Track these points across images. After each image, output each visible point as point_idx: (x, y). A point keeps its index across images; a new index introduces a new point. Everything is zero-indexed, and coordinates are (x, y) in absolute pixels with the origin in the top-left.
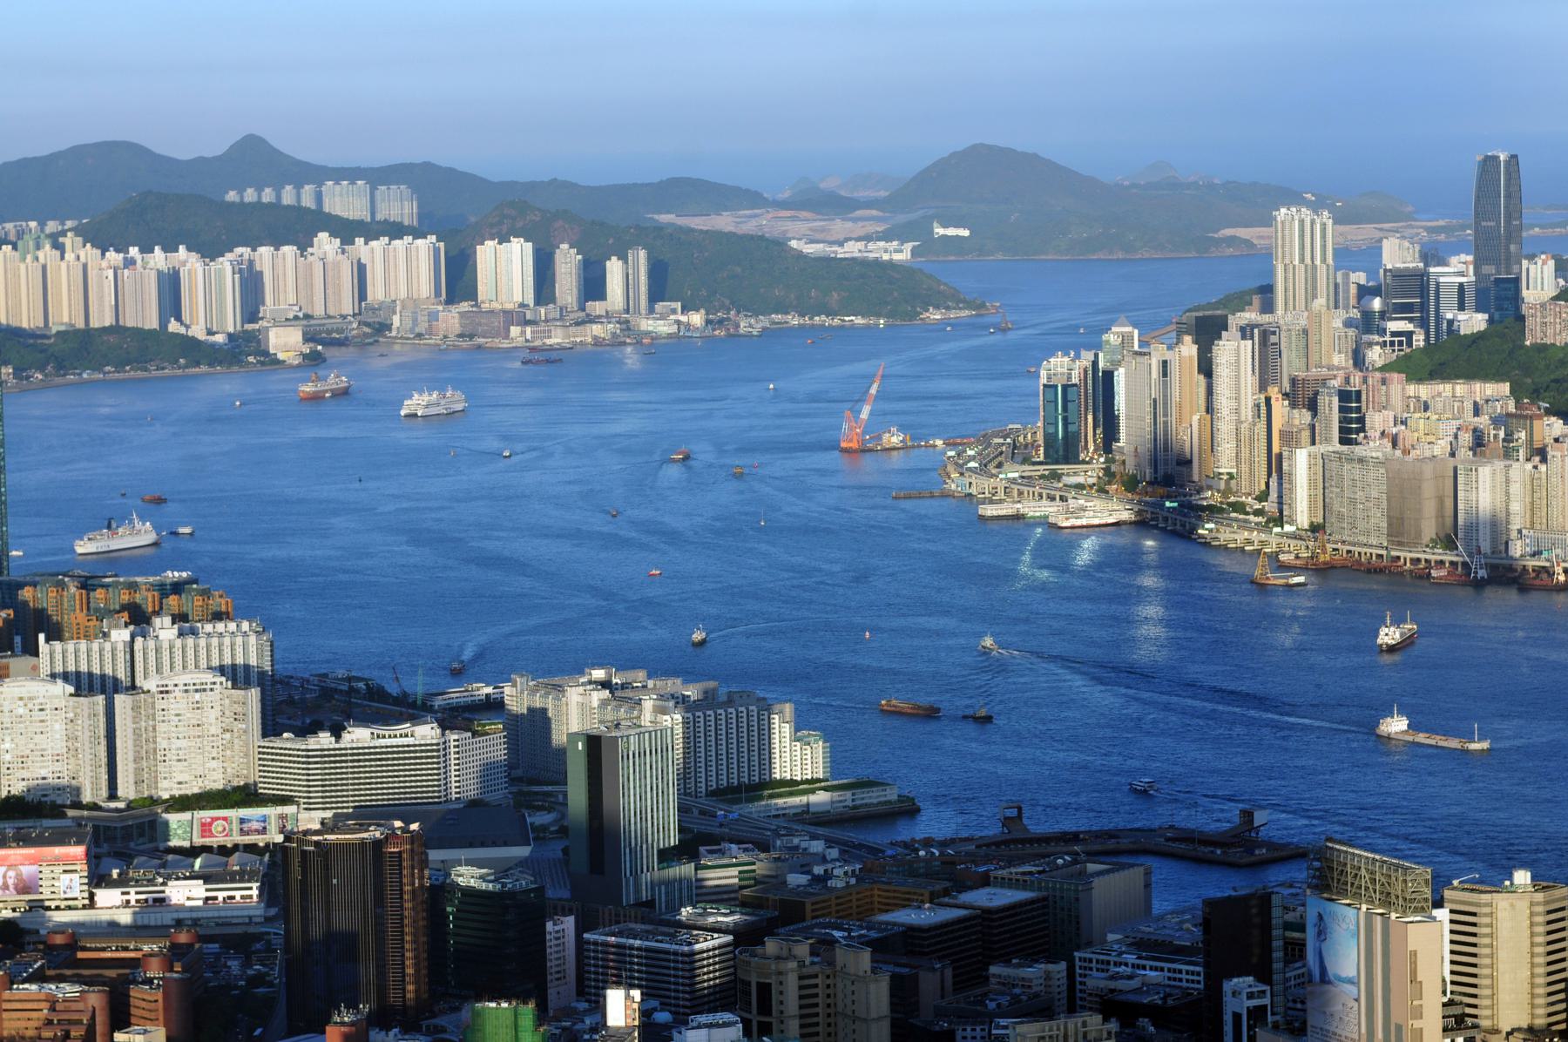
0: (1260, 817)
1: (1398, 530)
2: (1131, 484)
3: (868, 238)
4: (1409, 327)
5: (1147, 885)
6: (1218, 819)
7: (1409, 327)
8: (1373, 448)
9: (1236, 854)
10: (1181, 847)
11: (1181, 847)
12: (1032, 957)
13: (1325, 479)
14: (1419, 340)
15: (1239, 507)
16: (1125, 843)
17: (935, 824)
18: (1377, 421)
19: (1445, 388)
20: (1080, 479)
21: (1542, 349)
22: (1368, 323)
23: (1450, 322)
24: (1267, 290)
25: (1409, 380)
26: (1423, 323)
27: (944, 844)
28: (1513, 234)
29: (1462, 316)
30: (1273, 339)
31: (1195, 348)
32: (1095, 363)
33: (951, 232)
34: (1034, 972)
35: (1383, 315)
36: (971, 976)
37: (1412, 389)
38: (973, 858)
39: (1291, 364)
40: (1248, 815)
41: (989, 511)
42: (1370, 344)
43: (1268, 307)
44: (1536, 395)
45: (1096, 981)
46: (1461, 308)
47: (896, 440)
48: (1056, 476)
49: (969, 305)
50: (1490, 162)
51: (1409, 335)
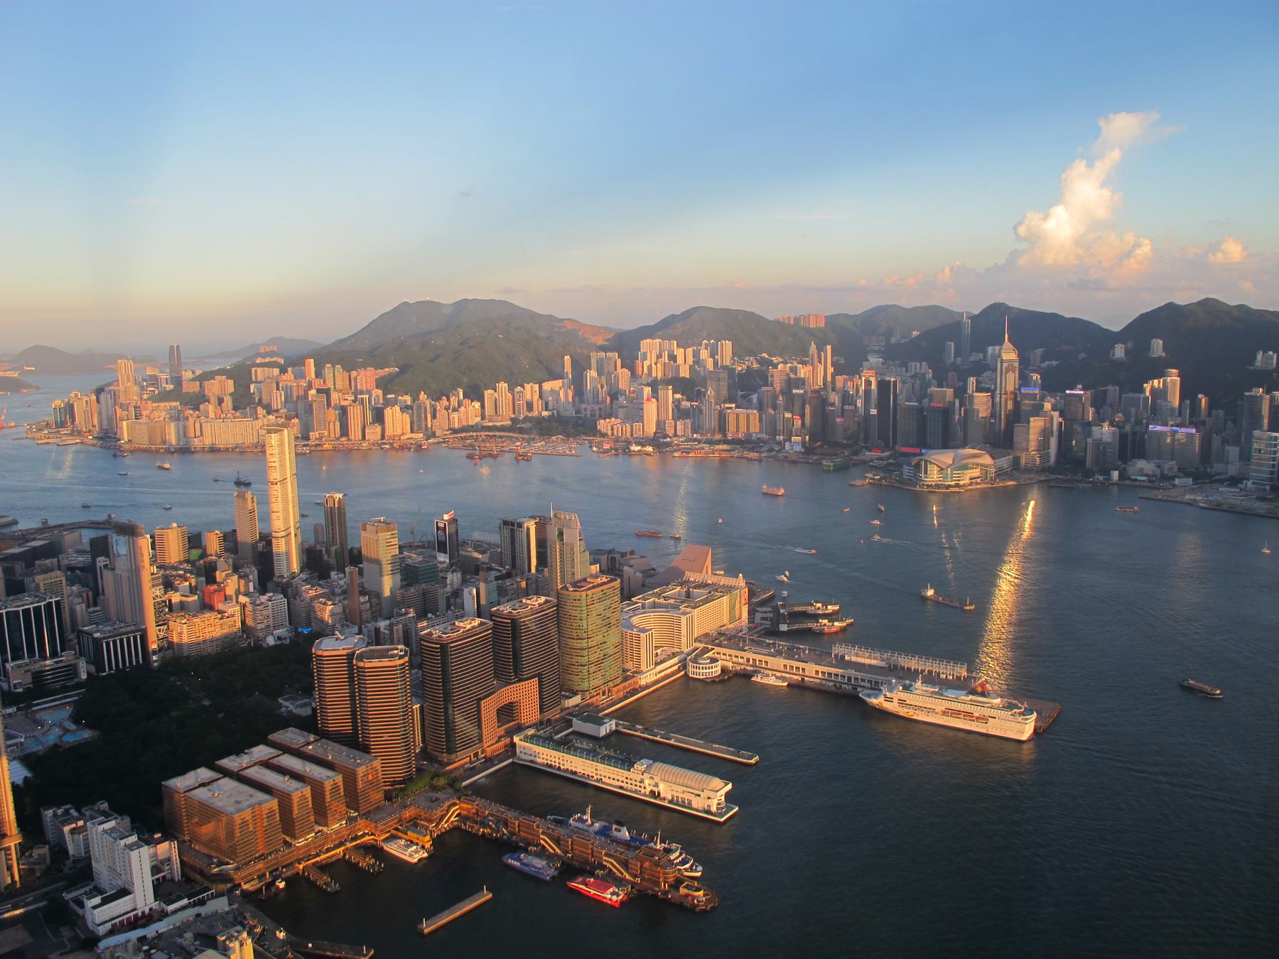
0: (113, 516)
1: (151, 441)
2: (80, 433)
3: (5, 371)
4: (153, 389)
5: (81, 536)
6: (102, 517)
7: (153, 389)
8: (144, 420)
9: (107, 526)
10: (92, 525)
11: (92, 525)
12: (47, 557)
13: (130, 429)
14: (156, 392)
15: (109, 437)
16: (77, 526)
17: (23, 525)
18: (144, 413)
19: (162, 404)
20: (66, 432)
21: (187, 393)
22: (142, 388)
23: (164, 388)
24: (118, 381)
25: (153, 402)
26: (158, 388)
27: (25, 531)
28: (180, 365)
29: (167, 386)
30: (117, 393)
31: (95, 397)
32: (68, 402)
33: (29, 368)
34: (48, 562)
35: (147, 387)
36: (30, 564)
37: (154, 405)
38: (32, 534)
39: (122, 400)
40: (110, 516)
41: (40, 442)
42: (144, 394)
43: (118, 385)
44: (186, 404)
45: (65, 562)
46: (167, 384)
47: (13, 424)
48: (59, 432)
49: (35, 388)
50: (172, 347)
51: (154, 391)
